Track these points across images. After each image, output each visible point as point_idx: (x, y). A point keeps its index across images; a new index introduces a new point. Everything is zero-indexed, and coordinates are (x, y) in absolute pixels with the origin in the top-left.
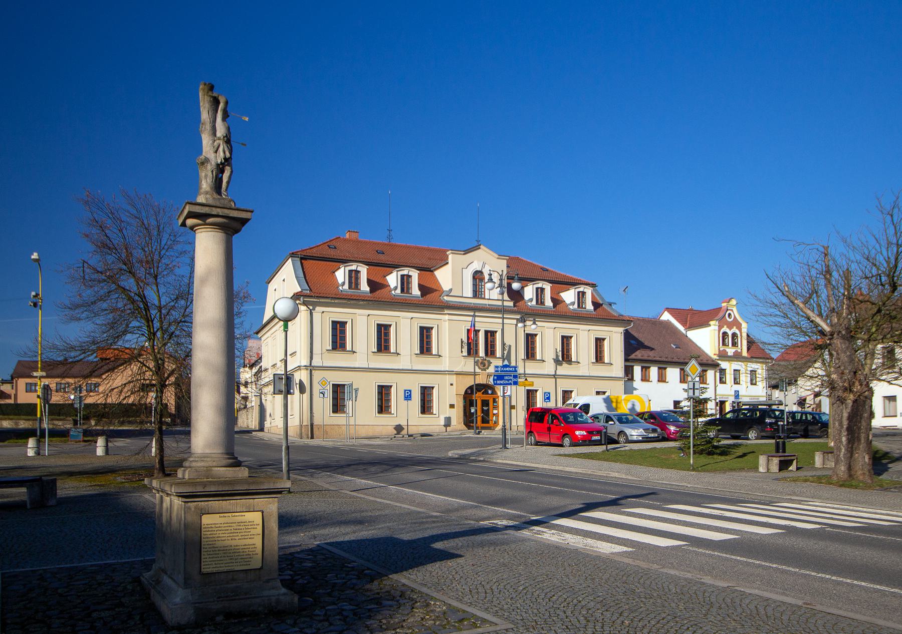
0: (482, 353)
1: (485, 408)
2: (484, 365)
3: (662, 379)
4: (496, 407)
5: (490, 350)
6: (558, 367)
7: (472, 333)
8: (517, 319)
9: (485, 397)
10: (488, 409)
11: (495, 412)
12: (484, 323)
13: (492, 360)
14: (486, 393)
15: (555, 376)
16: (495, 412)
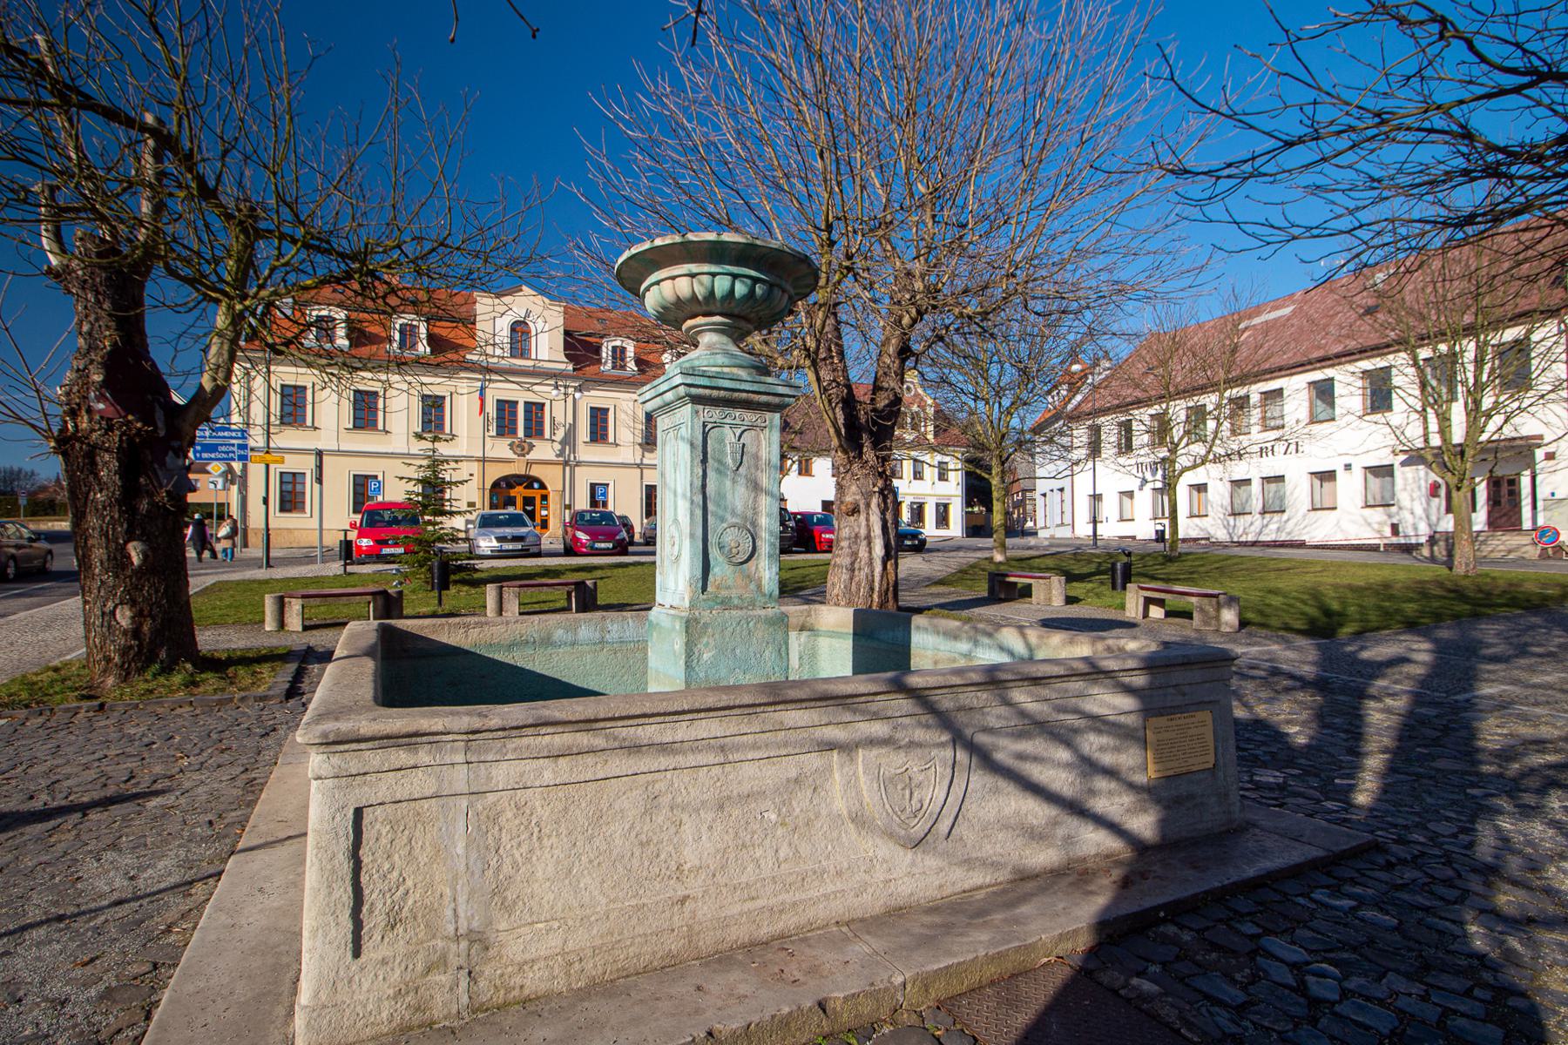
0: (521, 433)
1: (529, 508)
2: (522, 449)
3: (805, 470)
4: (547, 508)
5: (535, 428)
6: (646, 454)
7: (506, 409)
8: (575, 388)
9: (529, 493)
10: (534, 510)
11: (544, 513)
12: (518, 393)
13: (534, 442)
14: (530, 486)
15: (640, 466)
16: (544, 513)
